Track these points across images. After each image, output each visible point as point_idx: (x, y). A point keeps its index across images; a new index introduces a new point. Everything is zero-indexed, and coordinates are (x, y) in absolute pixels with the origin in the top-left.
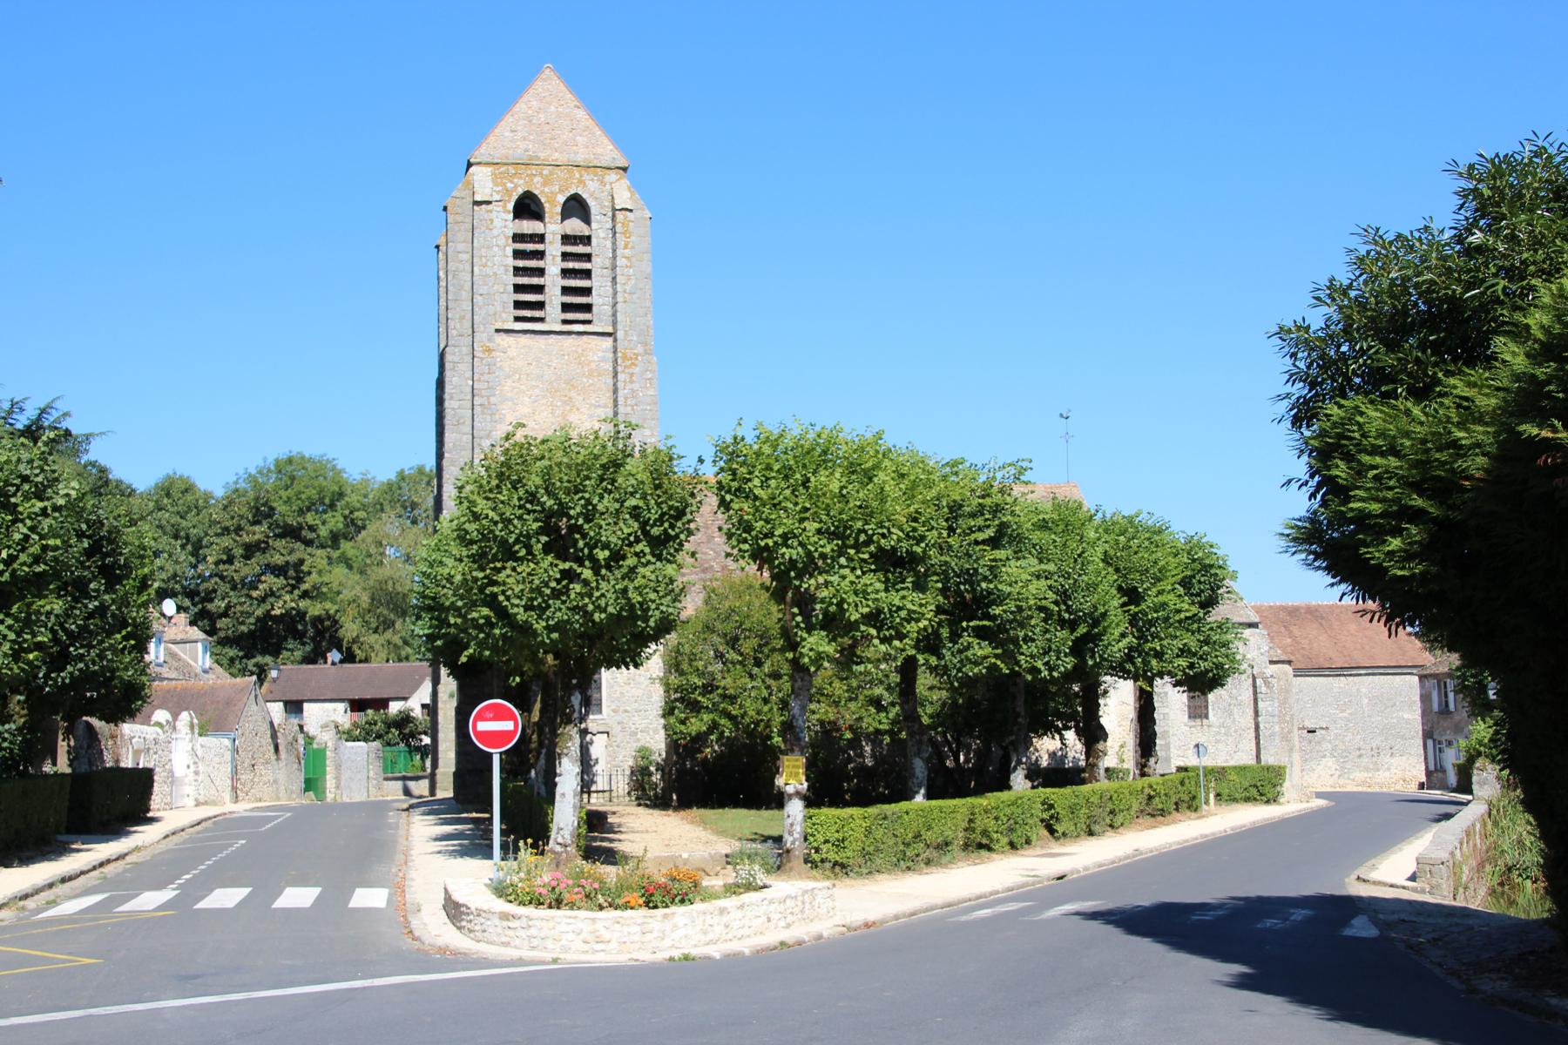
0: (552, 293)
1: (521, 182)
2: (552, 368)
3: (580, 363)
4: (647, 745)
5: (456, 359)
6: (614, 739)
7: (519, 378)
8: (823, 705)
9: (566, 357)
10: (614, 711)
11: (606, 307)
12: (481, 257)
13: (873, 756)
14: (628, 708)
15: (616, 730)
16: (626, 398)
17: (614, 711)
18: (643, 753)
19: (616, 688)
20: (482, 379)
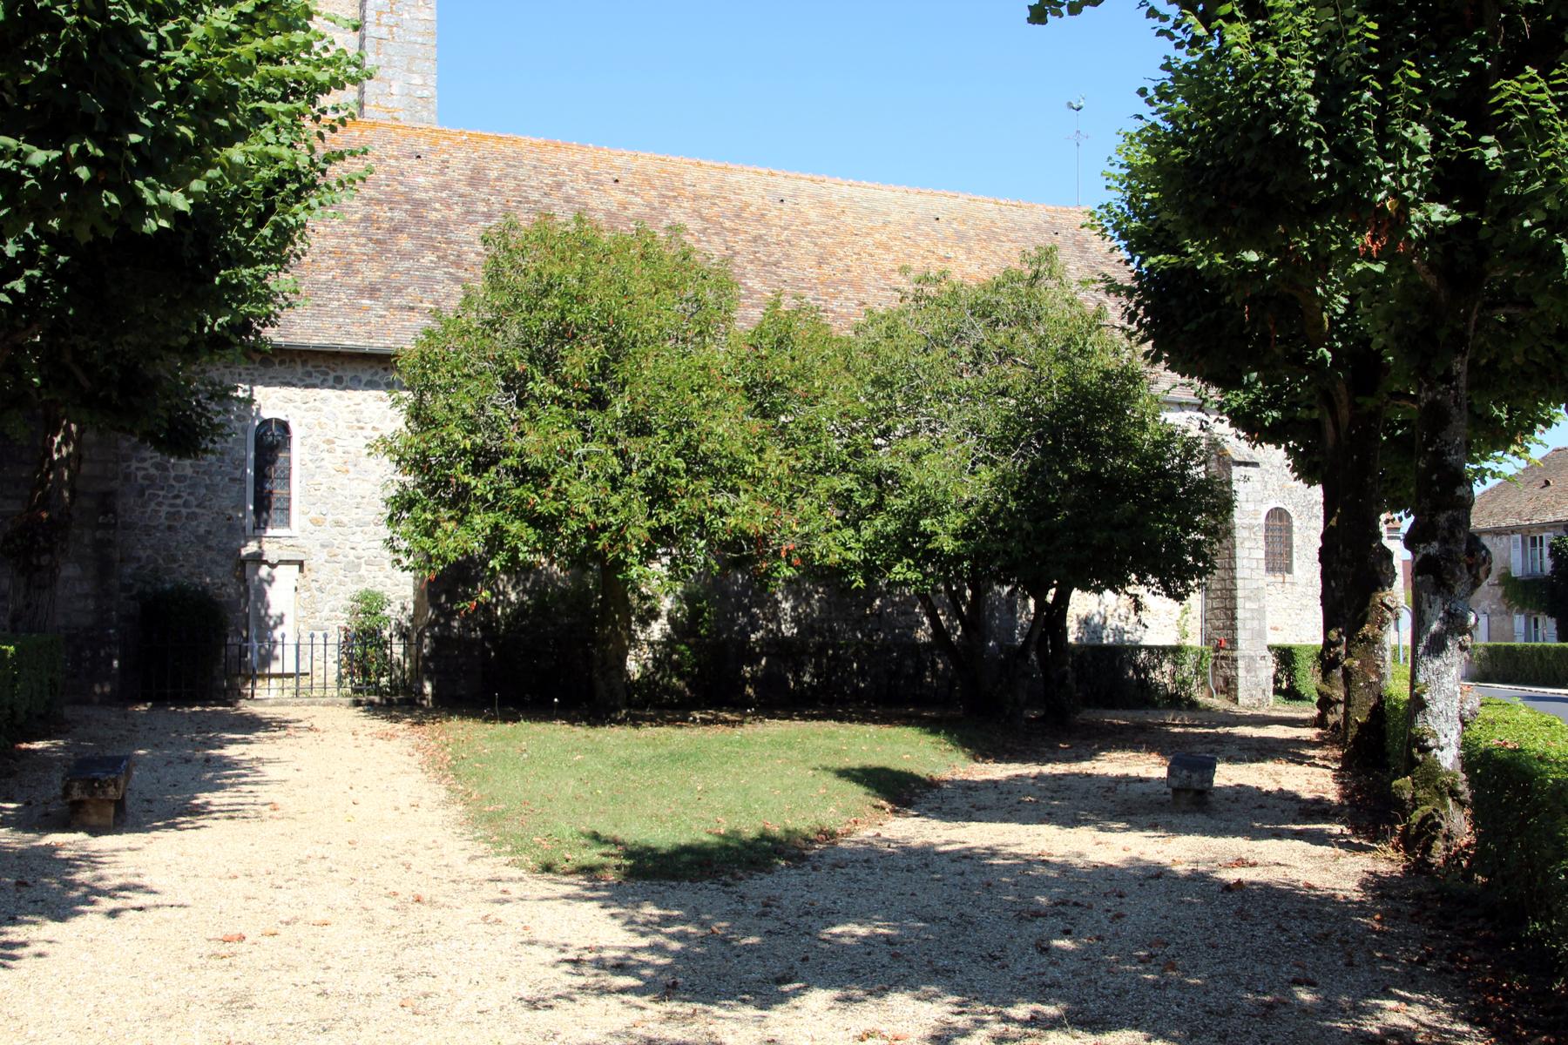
4: (378, 589)
6: (313, 576)
8: (744, 497)
10: (315, 522)
13: (796, 620)
14: (345, 520)
15: (315, 560)
16: (380, 13)
17: (315, 522)
18: (370, 604)
19: (318, 478)
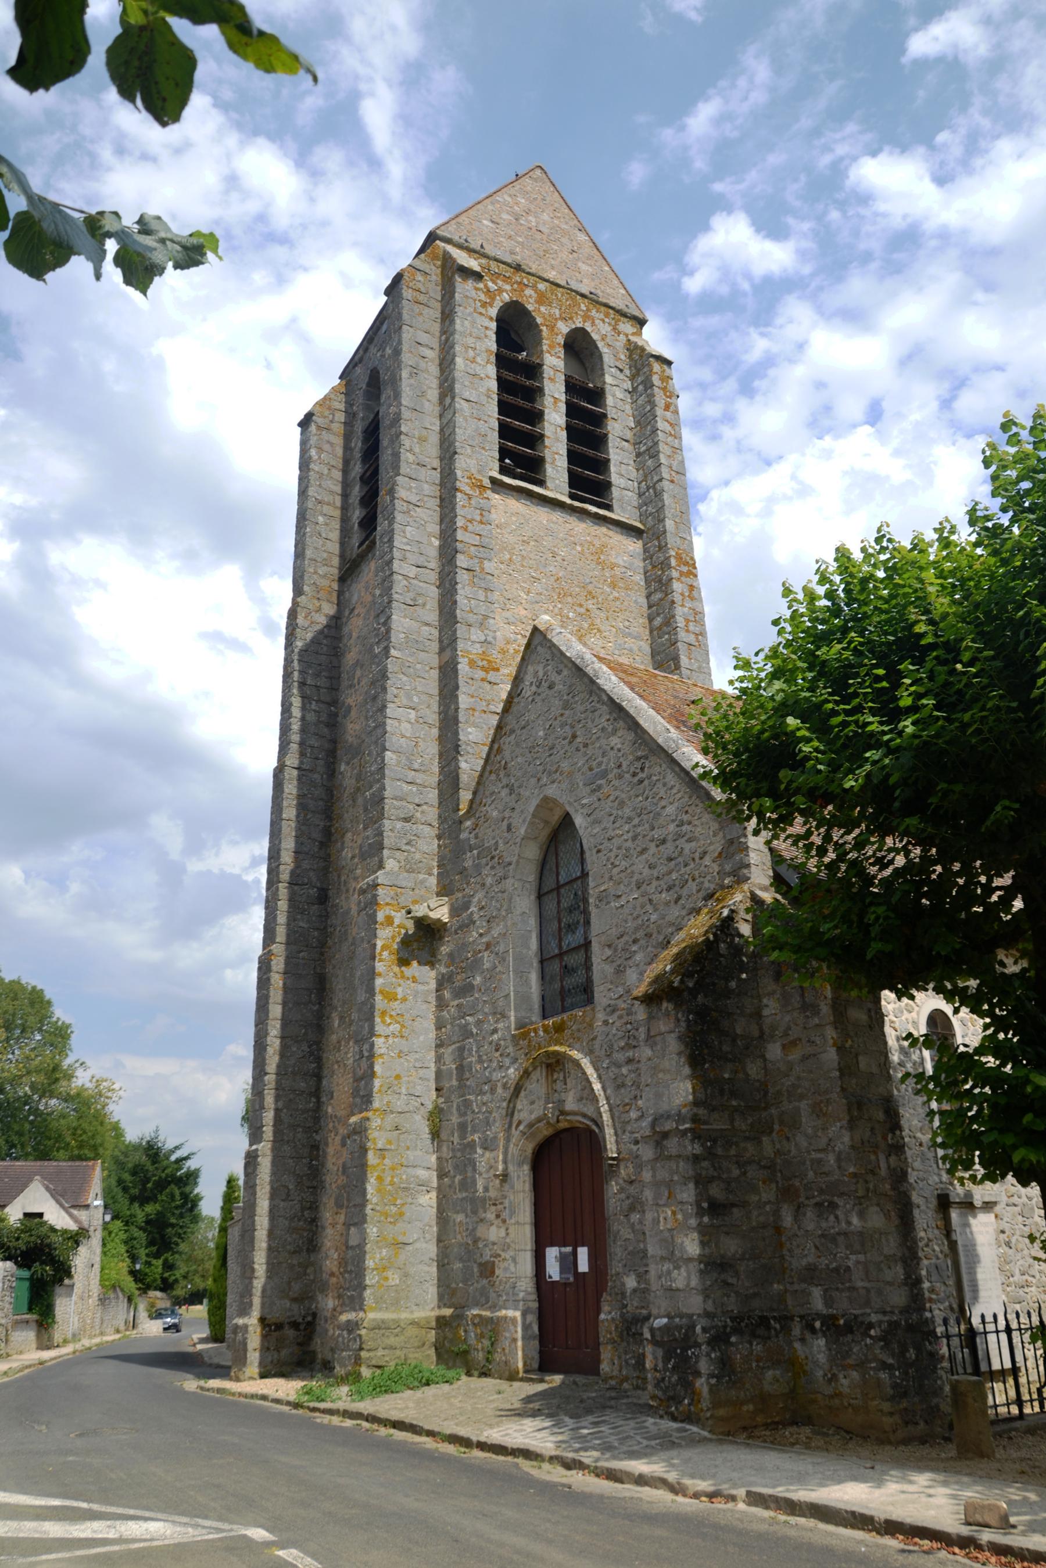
0: (554, 449)
1: (508, 287)
2: (558, 558)
3: (599, 563)
5: (413, 499)
7: (510, 559)
9: (579, 548)
11: (630, 494)
12: (467, 347)
16: (687, 621)
20: (470, 527)
